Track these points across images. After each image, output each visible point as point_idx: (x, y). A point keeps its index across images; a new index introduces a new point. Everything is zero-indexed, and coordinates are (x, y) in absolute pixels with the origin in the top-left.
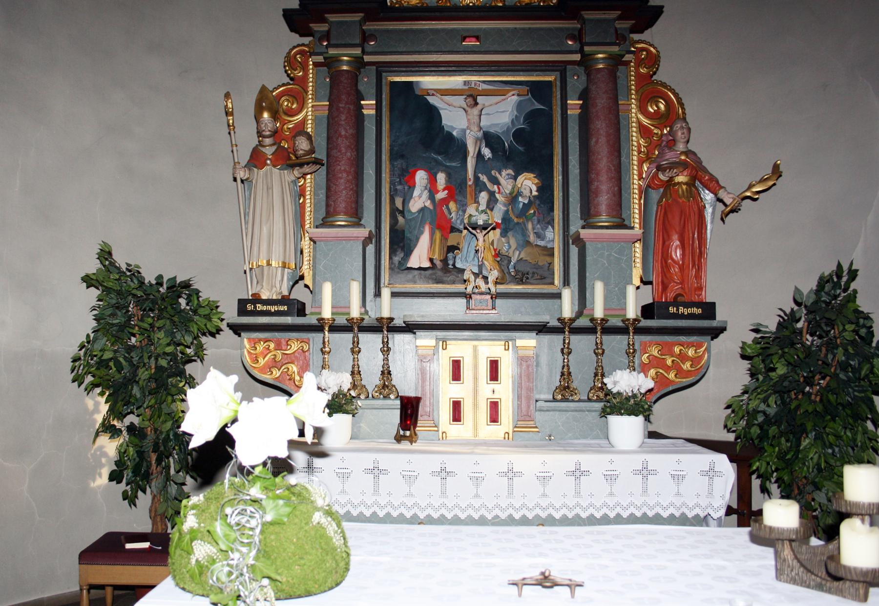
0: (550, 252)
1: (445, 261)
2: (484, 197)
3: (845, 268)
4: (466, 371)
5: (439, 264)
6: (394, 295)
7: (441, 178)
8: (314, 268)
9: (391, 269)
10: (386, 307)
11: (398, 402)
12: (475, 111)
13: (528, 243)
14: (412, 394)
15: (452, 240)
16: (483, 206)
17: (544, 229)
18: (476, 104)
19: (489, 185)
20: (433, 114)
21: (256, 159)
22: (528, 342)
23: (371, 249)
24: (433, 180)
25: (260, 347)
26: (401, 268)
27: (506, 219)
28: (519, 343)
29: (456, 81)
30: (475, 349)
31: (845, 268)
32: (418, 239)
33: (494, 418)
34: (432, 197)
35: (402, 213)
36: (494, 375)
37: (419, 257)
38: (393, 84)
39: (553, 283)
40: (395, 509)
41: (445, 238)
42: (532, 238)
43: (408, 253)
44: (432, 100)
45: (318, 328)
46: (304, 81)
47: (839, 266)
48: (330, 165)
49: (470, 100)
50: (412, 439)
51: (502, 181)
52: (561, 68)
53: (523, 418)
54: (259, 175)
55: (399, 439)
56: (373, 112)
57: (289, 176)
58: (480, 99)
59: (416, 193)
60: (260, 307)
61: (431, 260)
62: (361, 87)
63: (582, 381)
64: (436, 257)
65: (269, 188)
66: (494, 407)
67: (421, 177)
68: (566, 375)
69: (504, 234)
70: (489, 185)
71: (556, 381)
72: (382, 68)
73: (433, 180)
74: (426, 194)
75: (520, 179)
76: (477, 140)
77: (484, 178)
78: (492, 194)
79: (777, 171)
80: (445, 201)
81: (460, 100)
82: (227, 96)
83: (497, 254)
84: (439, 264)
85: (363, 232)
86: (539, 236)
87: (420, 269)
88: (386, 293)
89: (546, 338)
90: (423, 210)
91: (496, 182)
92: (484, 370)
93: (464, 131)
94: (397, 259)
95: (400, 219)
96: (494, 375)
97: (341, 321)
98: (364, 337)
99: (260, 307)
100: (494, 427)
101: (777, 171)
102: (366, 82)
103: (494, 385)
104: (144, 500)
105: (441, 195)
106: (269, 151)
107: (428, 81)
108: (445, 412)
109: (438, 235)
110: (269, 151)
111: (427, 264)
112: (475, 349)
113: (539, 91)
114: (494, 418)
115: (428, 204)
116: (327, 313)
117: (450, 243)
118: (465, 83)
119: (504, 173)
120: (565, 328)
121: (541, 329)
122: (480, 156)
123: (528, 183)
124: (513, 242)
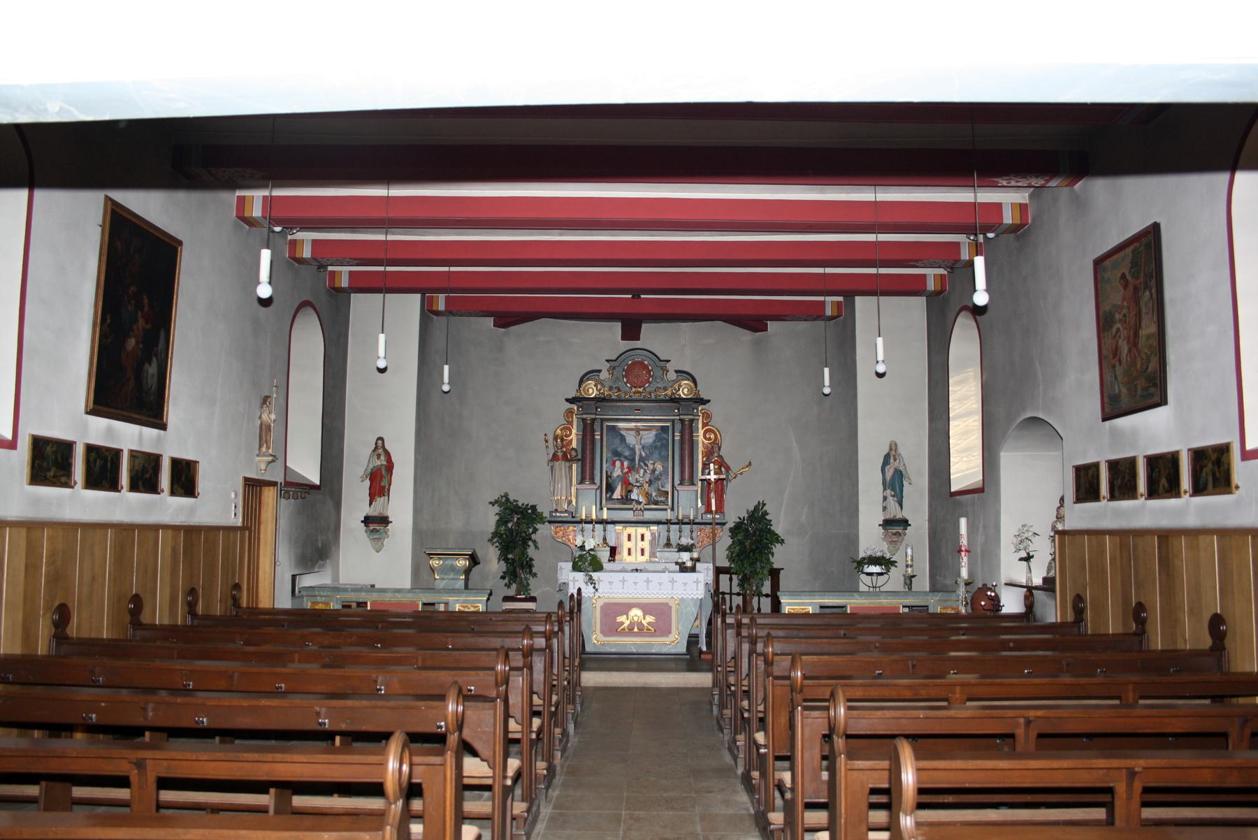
0: (667, 493)
1: (627, 496)
2: (642, 471)
3: (761, 502)
4: (633, 538)
5: (624, 497)
6: (608, 509)
7: (626, 464)
8: (577, 498)
9: (606, 499)
10: (605, 515)
11: (609, 548)
12: (639, 437)
13: (659, 490)
14: (614, 545)
15: (630, 488)
16: (642, 475)
17: (665, 483)
18: (639, 434)
19: (644, 467)
20: (623, 438)
21: (555, 457)
22: (654, 528)
23: (598, 491)
24: (622, 464)
25: (558, 529)
26: (610, 499)
27: (650, 480)
28: (652, 528)
29: (633, 425)
30: (636, 530)
31: (761, 502)
32: (616, 488)
33: (643, 554)
34: (622, 471)
35: (610, 477)
36: (643, 539)
37: (617, 495)
38: (607, 426)
39: (668, 505)
40: (606, 594)
41: (626, 487)
42: (660, 487)
43: (613, 492)
44: (622, 432)
45: (581, 522)
46: (571, 423)
47: (759, 502)
48: (583, 460)
49: (637, 433)
50: (614, 561)
51: (649, 465)
52: (673, 421)
53: (653, 554)
54: (557, 464)
55: (609, 561)
56: (599, 437)
57: (567, 464)
58: (641, 432)
59: (616, 470)
60: (558, 514)
61: (621, 496)
62: (595, 427)
63: (674, 541)
64: (624, 494)
65: (561, 469)
66: (643, 550)
67: (618, 464)
68: (668, 539)
69: (649, 486)
70: (644, 467)
71: (665, 542)
72: (602, 420)
73: (622, 464)
74: (620, 470)
75: (656, 464)
76: (640, 449)
77: (642, 464)
78: (645, 471)
79: (750, 464)
80: (627, 473)
81: (633, 433)
82: (546, 435)
83: (647, 493)
84: (624, 497)
85: (596, 487)
86: (662, 487)
87: (617, 499)
88: (605, 509)
89: (661, 526)
90: (617, 476)
91: (646, 465)
92: (639, 537)
93: (635, 445)
94: (608, 496)
95: (610, 479)
96: (643, 539)
97: (589, 519)
98: (597, 526)
99: (558, 514)
100: (643, 557)
101: (750, 464)
102: (597, 426)
103: (643, 543)
104: (514, 586)
105: (626, 470)
106: (560, 454)
107: (621, 425)
108: (625, 552)
109: (624, 486)
110: (560, 454)
111: (620, 497)
112: (636, 530)
113: (664, 429)
114: (643, 554)
115: (621, 474)
116: (584, 517)
117: (629, 489)
118: (635, 426)
119: (650, 462)
120: (668, 522)
121: (658, 523)
122: (641, 455)
123: (659, 466)
124: (653, 489)
